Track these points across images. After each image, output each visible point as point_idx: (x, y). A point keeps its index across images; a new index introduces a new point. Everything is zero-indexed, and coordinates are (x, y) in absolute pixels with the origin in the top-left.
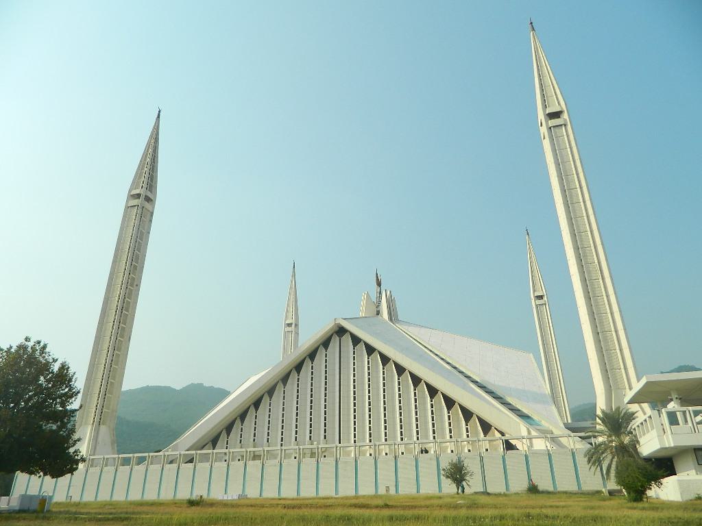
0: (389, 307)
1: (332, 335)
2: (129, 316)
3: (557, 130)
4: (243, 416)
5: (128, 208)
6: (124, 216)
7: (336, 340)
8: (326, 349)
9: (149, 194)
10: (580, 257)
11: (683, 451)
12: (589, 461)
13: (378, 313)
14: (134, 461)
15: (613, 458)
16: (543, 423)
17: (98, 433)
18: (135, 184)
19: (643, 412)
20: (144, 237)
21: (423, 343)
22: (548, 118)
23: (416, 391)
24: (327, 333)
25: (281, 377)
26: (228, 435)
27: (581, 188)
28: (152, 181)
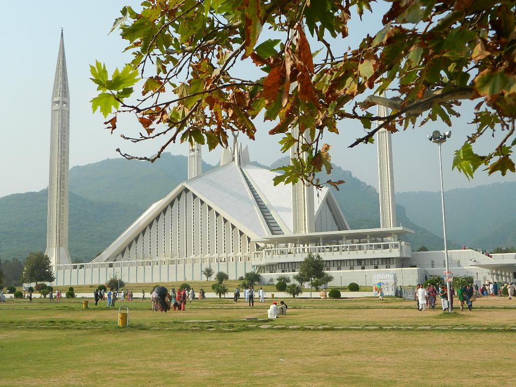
0: (239, 156)
1: (182, 192)
2: (65, 183)
4: (137, 239)
5: (53, 111)
6: (52, 118)
7: (184, 193)
8: (179, 200)
9: (65, 100)
13: (234, 159)
14: (78, 267)
17: (59, 252)
18: (55, 94)
20: (66, 132)
25: (156, 216)
26: (130, 249)
28: (65, 89)
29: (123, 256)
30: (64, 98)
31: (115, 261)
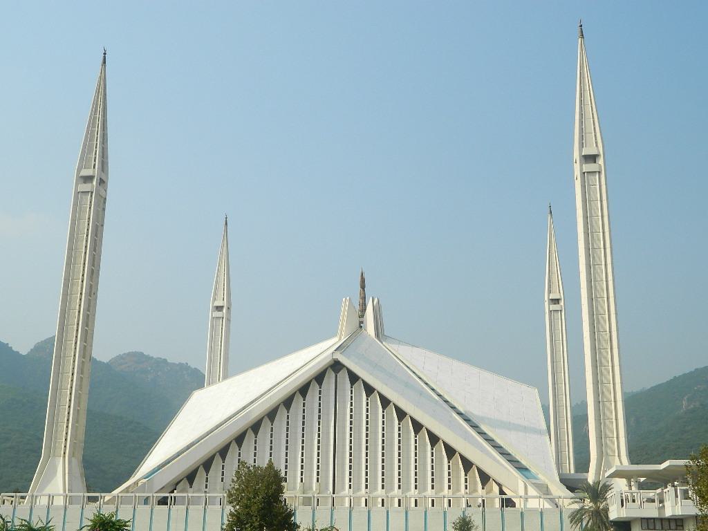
3: (591, 177)
5: (77, 193)
6: (75, 204)
7: (330, 376)
8: (320, 384)
10: (593, 324)
11: (636, 519)
12: (571, 522)
15: (590, 520)
16: (540, 476)
19: (620, 485)
21: (417, 372)
22: (583, 159)
23: (417, 438)
24: (321, 368)
27: (605, 249)
29: (191, 483)
30: (103, 174)
31: (172, 492)
